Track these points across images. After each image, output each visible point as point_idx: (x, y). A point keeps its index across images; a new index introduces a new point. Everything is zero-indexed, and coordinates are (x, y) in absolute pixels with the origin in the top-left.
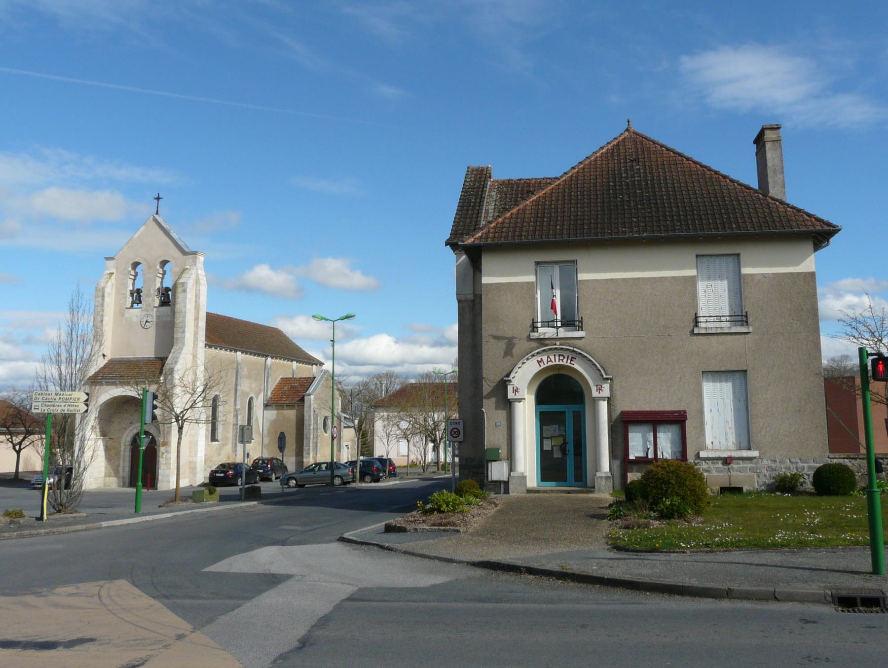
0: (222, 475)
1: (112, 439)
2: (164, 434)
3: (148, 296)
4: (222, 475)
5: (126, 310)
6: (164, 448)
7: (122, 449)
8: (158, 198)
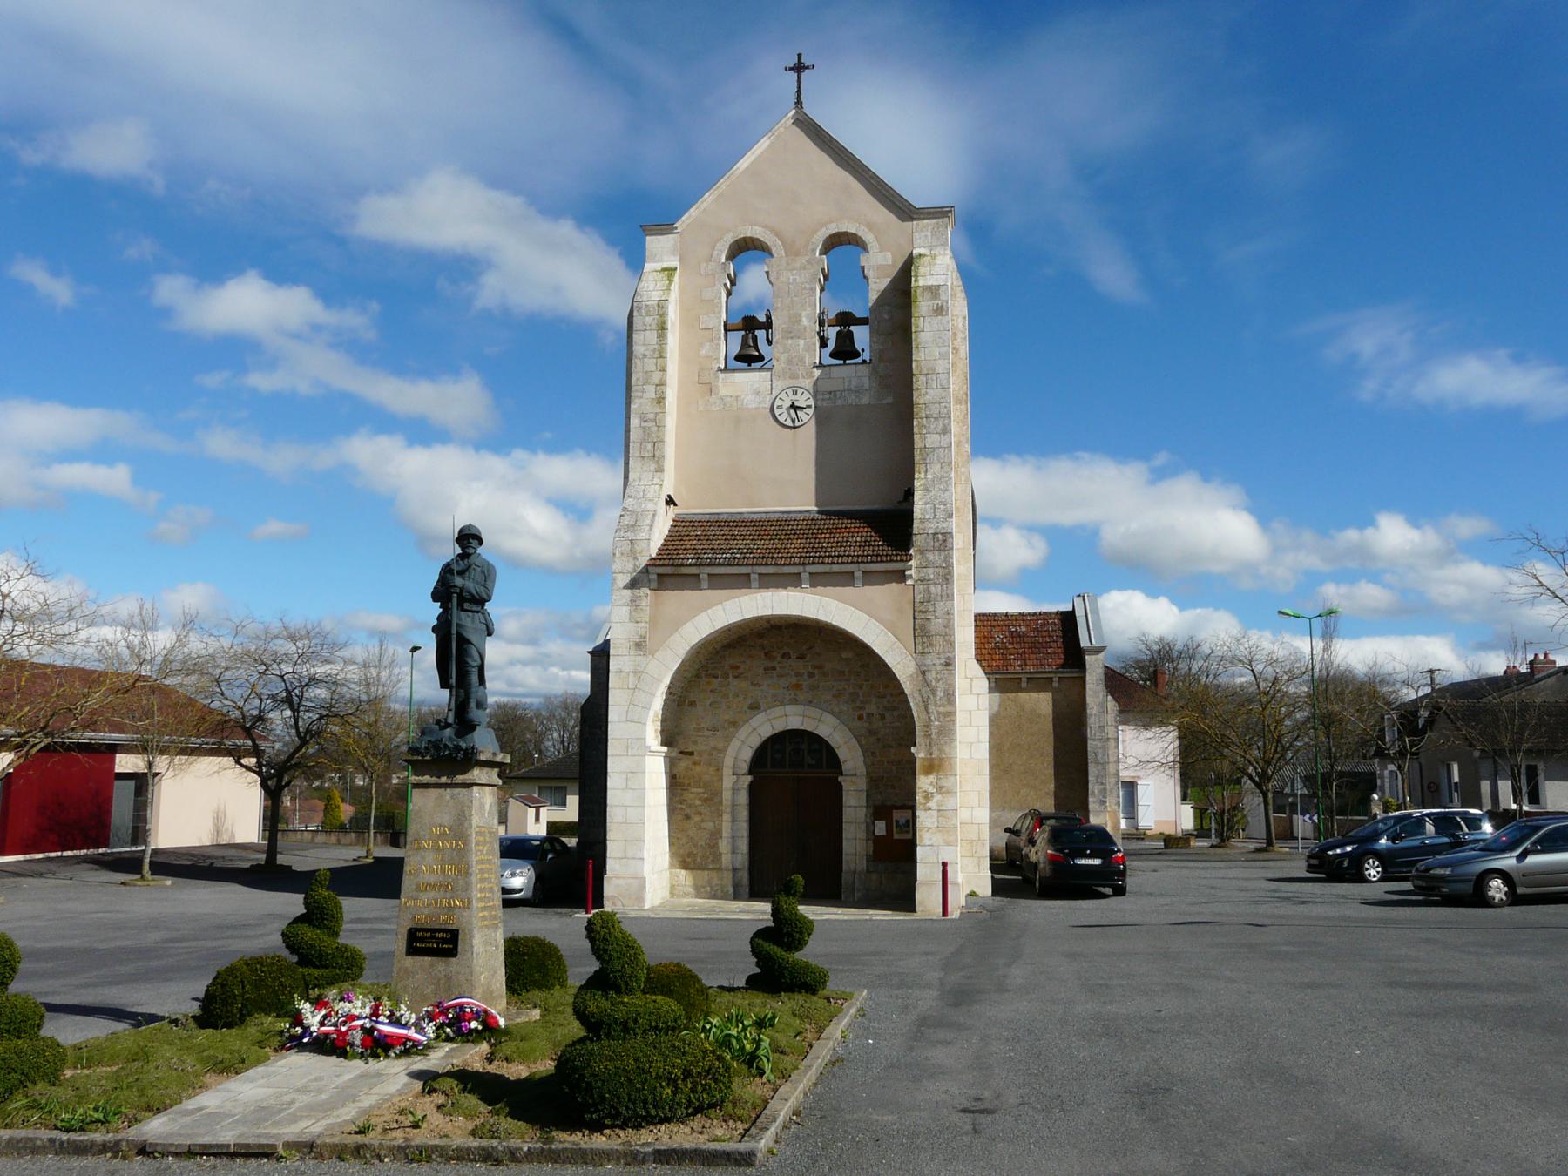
0: (1098, 862)
1: (692, 754)
2: (927, 736)
3: (791, 333)
4: (1098, 862)
5: (721, 375)
6: (932, 778)
7: (728, 782)
8: (799, 68)
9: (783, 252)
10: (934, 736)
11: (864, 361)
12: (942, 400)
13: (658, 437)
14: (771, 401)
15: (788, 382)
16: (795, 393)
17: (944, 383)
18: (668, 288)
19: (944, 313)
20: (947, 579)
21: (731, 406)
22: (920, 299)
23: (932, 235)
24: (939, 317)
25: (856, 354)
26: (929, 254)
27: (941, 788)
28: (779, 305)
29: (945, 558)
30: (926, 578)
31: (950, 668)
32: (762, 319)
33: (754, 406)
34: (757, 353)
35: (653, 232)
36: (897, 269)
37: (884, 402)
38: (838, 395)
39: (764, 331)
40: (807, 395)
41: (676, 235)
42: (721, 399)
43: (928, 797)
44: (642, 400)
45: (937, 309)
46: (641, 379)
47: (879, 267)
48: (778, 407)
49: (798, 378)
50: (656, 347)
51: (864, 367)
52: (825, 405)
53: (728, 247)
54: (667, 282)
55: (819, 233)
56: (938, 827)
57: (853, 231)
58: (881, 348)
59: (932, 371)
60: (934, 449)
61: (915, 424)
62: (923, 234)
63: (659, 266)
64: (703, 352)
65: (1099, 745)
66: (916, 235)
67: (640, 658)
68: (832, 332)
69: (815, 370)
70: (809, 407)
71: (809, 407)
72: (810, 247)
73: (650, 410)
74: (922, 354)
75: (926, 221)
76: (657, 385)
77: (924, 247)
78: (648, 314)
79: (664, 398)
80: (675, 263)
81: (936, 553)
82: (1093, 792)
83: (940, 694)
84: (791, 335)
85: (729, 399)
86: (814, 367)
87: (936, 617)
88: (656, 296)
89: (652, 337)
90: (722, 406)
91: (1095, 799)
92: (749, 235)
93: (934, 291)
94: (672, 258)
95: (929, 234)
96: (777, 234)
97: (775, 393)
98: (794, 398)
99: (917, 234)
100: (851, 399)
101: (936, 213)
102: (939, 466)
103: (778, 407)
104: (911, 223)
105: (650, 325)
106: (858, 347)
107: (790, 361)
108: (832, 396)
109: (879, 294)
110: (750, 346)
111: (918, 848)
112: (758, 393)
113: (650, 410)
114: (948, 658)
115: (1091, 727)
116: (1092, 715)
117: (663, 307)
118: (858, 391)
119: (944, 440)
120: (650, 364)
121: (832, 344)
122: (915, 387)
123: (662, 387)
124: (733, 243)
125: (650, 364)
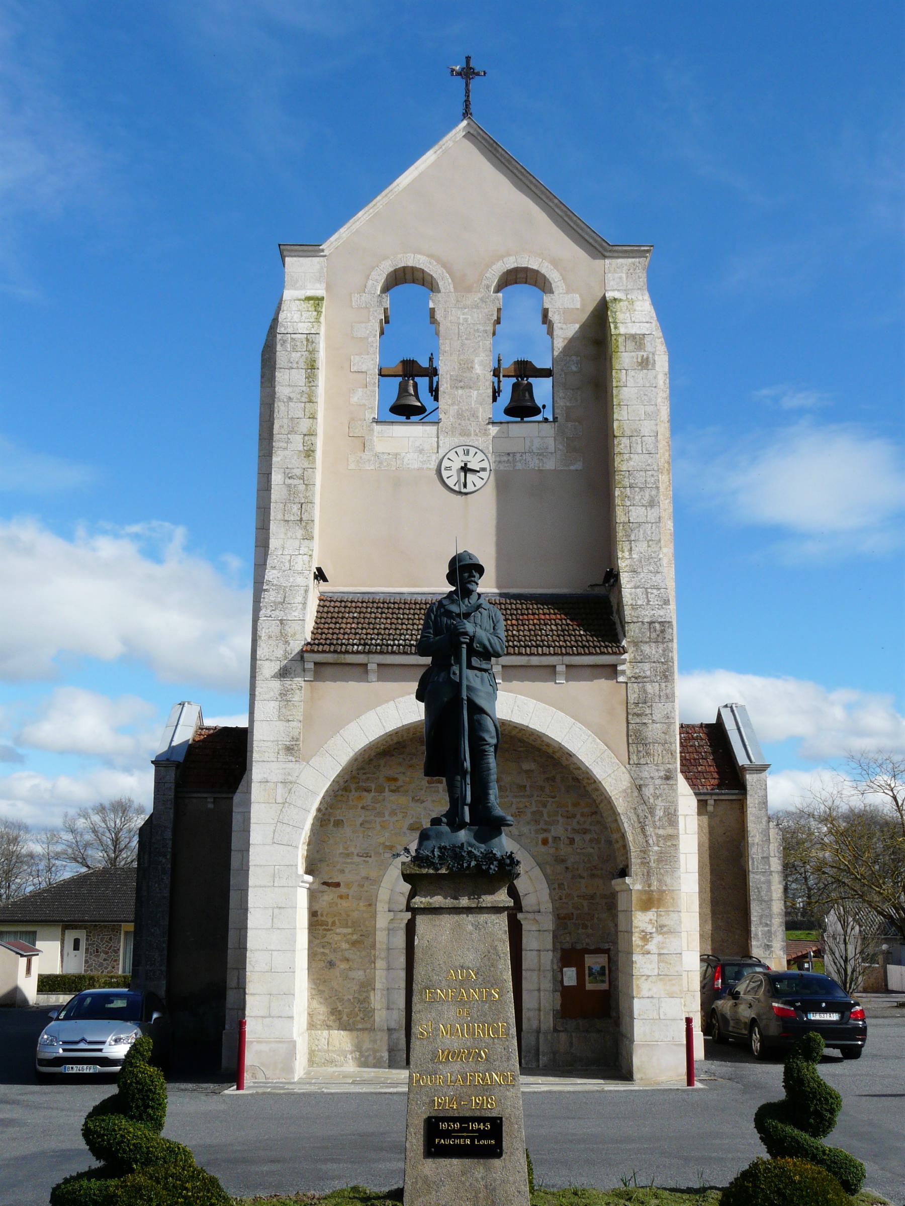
0: (835, 1017)
1: (338, 885)
2: (645, 863)
3: (459, 382)
4: (835, 1017)
5: (377, 428)
6: (651, 915)
7: (382, 920)
8: (468, 73)
9: (452, 286)
10: (653, 864)
11: (546, 420)
12: (648, 468)
13: (306, 497)
14: (437, 461)
15: (457, 440)
16: (467, 453)
17: (651, 447)
18: (317, 320)
19: (650, 367)
20: (666, 677)
21: (388, 465)
22: (622, 348)
23: (627, 277)
24: (645, 371)
25: (535, 411)
26: (624, 298)
27: (662, 926)
28: (447, 349)
29: (664, 651)
30: (642, 674)
31: (671, 782)
32: (425, 364)
33: (416, 466)
34: (419, 404)
35: (293, 254)
36: (588, 314)
37: (572, 468)
38: (518, 457)
39: (427, 379)
40: (480, 456)
41: (322, 259)
42: (377, 455)
43: (646, 937)
44: (286, 452)
45: (642, 362)
46: (285, 426)
47: (566, 311)
48: (447, 468)
49: (469, 435)
50: (304, 389)
51: (545, 425)
52: (502, 468)
53: (385, 276)
54: (315, 313)
55: (494, 267)
56: (659, 975)
57: (535, 267)
58: (568, 404)
59: (636, 434)
60: (639, 524)
61: (616, 495)
62: (617, 275)
63: (302, 294)
64: (355, 399)
65: (763, 879)
66: (609, 276)
67: (291, 765)
68: (507, 385)
69: (490, 426)
70: (484, 469)
71: (484, 469)
72: (485, 282)
73: (297, 464)
74: (624, 413)
75: (620, 261)
76: (305, 435)
77: (618, 290)
78: (294, 350)
79: (313, 451)
80: (320, 292)
81: (653, 645)
82: (756, 935)
83: (659, 813)
84: (462, 384)
85: (386, 457)
86: (489, 423)
87: (654, 722)
88: (303, 328)
89: (299, 377)
90: (377, 465)
91: (758, 943)
92: (410, 264)
93: (638, 340)
94: (318, 285)
95: (624, 276)
96: (444, 265)
97: (442, 452)
98: (466, 458)
99: (610, 275)
100: (534, 463)
101: (632, 251)
102: (645, 544)
103: (447, 468)
104: (602, 261)
105: (297, 363)
106: (539, 403)
107: (460, 415)
108: (510, 458)
109: (566, 341)
110: (411, 395)
111: (636, 1001)
112: (421, 451)
113: (297, 464)
114: (669, 771)
115: (753, 859)
116: (754, 844)
117: (313, 342)
118: (542, 454)
119: (652, 514)
120: (296, 409)
121: (505, 398)
122: (617, 450)
123: (312, 438)
124: (391, 272)
125: (296, 409)
